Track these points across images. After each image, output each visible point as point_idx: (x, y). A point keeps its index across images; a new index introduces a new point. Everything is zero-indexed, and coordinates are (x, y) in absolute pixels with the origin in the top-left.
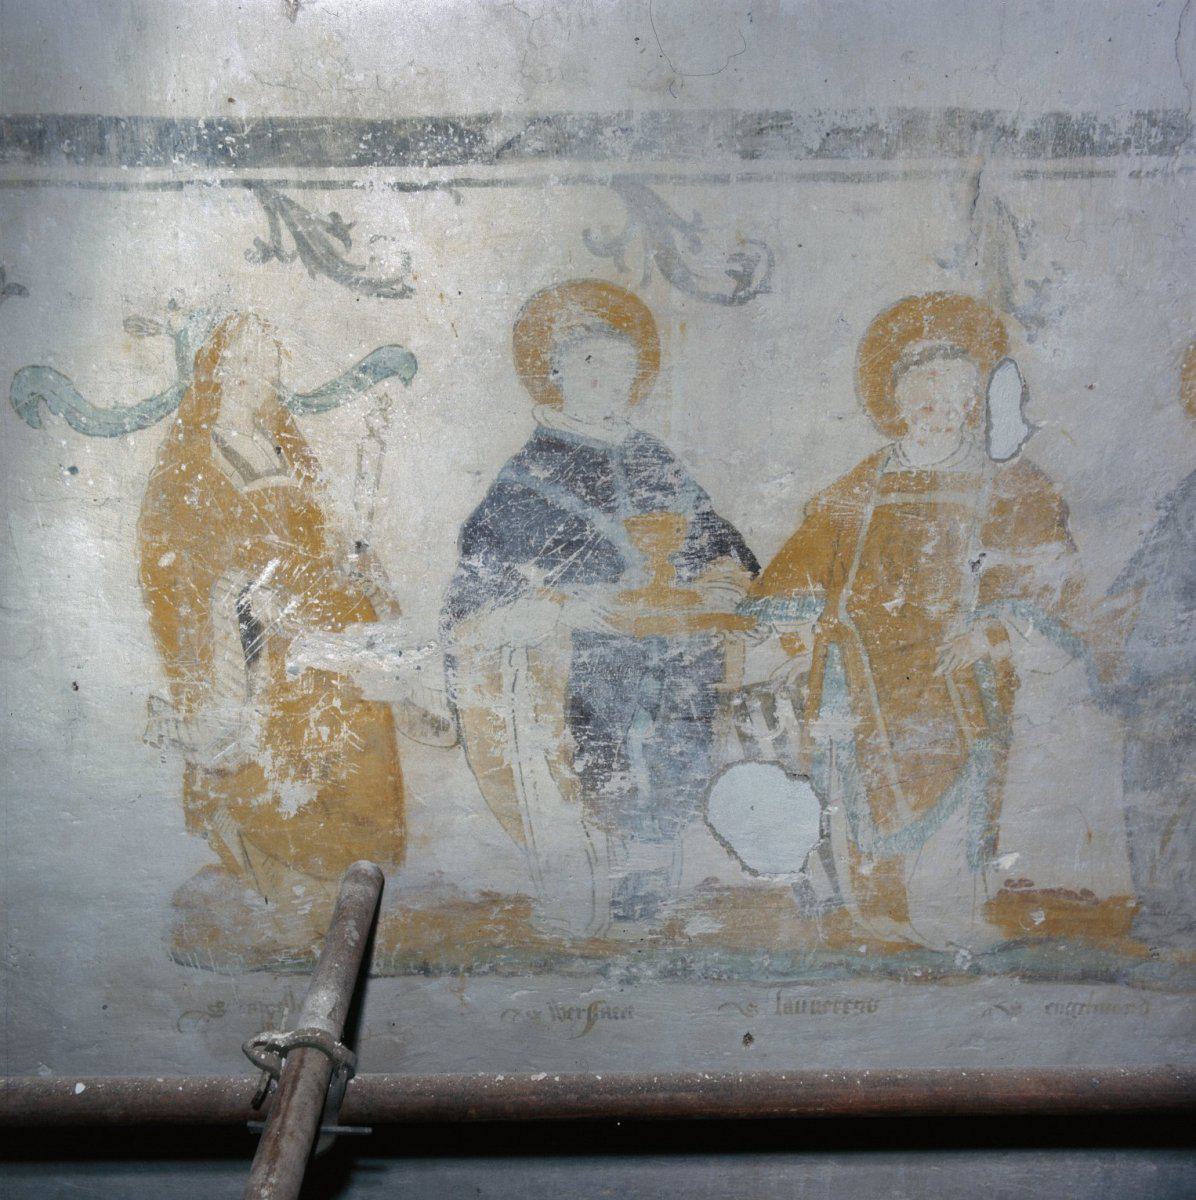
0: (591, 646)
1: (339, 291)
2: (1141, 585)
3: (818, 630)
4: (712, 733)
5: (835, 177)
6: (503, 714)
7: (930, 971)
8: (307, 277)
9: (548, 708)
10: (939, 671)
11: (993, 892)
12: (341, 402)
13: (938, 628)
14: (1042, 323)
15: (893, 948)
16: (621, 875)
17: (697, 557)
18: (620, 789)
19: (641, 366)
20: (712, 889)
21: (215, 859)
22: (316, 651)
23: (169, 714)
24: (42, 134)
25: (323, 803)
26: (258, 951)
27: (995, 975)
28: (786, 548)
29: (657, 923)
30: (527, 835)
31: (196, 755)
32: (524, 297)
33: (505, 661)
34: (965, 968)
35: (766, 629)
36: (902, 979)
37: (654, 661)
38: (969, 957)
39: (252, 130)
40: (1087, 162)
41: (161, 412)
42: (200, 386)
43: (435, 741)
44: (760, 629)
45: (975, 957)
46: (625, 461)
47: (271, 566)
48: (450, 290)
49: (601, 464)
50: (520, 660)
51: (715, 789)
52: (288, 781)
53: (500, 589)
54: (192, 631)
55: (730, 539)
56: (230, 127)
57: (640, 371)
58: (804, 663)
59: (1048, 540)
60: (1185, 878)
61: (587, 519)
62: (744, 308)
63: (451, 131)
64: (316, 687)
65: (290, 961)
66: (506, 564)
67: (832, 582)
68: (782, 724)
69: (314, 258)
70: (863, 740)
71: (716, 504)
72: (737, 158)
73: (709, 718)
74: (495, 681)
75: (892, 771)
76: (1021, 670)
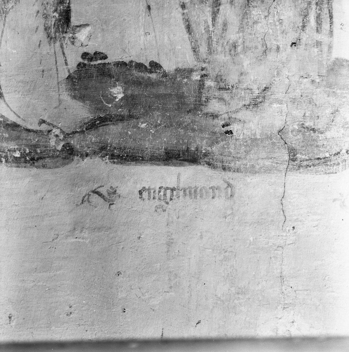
7: (28, 151)
27: (87, 155)
34: (59, 148)
36: (3, 160)
38: (62, 137)
45: (67, 135)
60: (239, 49)
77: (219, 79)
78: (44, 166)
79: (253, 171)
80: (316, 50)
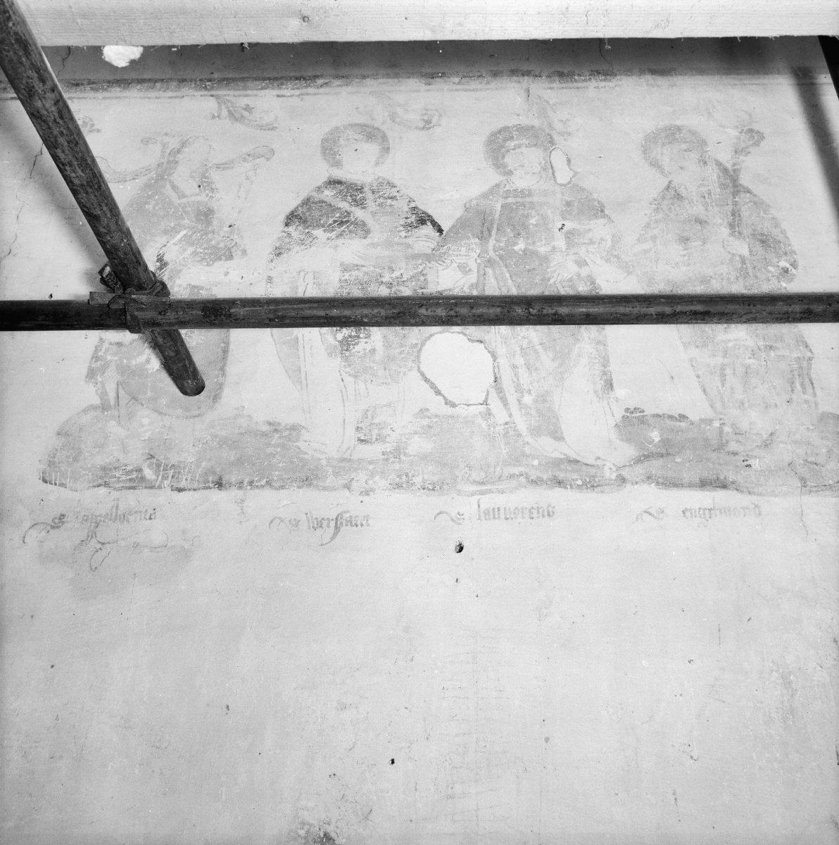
2: (654, 238)
3: (479, 261)
7: (588, 480)
10: (552, 281)
13: (545, 259)
15: (557, 463)
18: (364, 349)
21: (97, 401)
26: (104, 469)
27: (637, 483)
29: (388, 445)
37: (386, 279)
38: (614, 469)
42: (169, 162)
47: (182, 233)
50: (310, 276)
51: (425, 348)
53: (302, 242)
55: (427, 218)
65: (124, 478)
66: (307, 231)
67: (483, 237)
77: (733, 425)
78: (602, 492)
79: (773, 494)
80: (806, 406)
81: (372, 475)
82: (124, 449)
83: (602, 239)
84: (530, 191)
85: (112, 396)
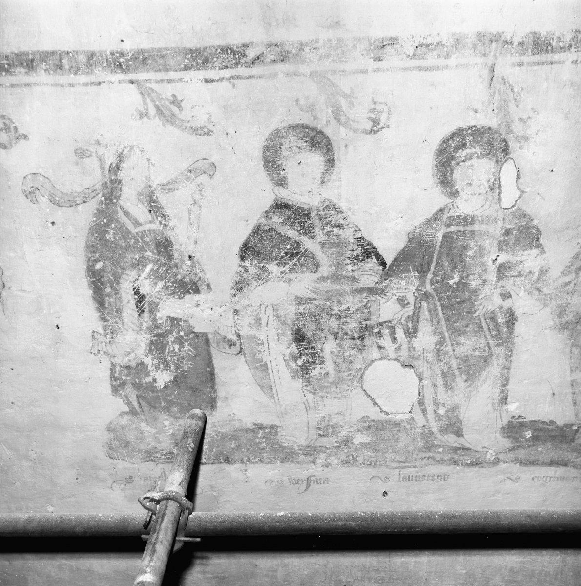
0: (304, 304)
1: (177, 132)
3: (416, 294)
4: (364, 346)
5: (420, 69)
6: (262, 337)
7: (474, 460)
8: (161, 126)
9: (284, 334)
10: (476, 314)
11: (505, 422)
12: (180, 187)
13: (476, 292)
14: (527, 139)
15: (456, 450)
16: (321, 415)
17: (356, 259)
18: (320, 373)
19: (326, 166)
20: (366, 422)
22: (171, 307)
23: (102, 339)
24: (32, 60)
25: (177, 381)
26: (147, 452)
27: (507, 462)
28: (399, 254)
30: (275, 395)
31: (116, 359)
32: (267, 133)
33: (263, 311)
34: (492, 459)
35: (390, 295)
36: (461, 464)
37: (335, 311)
38: (494, 454)
39: (133, 55)
40: (549, 57)
41: (94, 195)
42: (112, 181)
43: (229, 351)
44: (387, 294)
45: (497, 453)
46: (319, 213)
47: (150, 267)
48: (231, 131)
49: (307, 215)
50: (270, 311)
51: (367, 372)
52: (159, 371)
53: (259, 277)
54: (112, 300)
55: (371, 250)
56: (122, 55)
57: (326, 169)
58: (409, 310)
59: (531, 247)
61: (301, 242)
62: (376, 136)
63: (229, 52)
64: (172, 326)
65: (163, 457)
66: (262, 265)
67: (423, 272)
68: (399, 341)
69: (165, 117)
70: (439, 348)
71: (364, 233)
72: (371, 61)
73: (363, 338)
74: (258, 322)
75: (454, 364)
76: (518, 313)
78: (482, 467)
81: (330, 455)
82: (157, 440)
83: (530, 272)
84: (473, 218)
85: (136, 404)
